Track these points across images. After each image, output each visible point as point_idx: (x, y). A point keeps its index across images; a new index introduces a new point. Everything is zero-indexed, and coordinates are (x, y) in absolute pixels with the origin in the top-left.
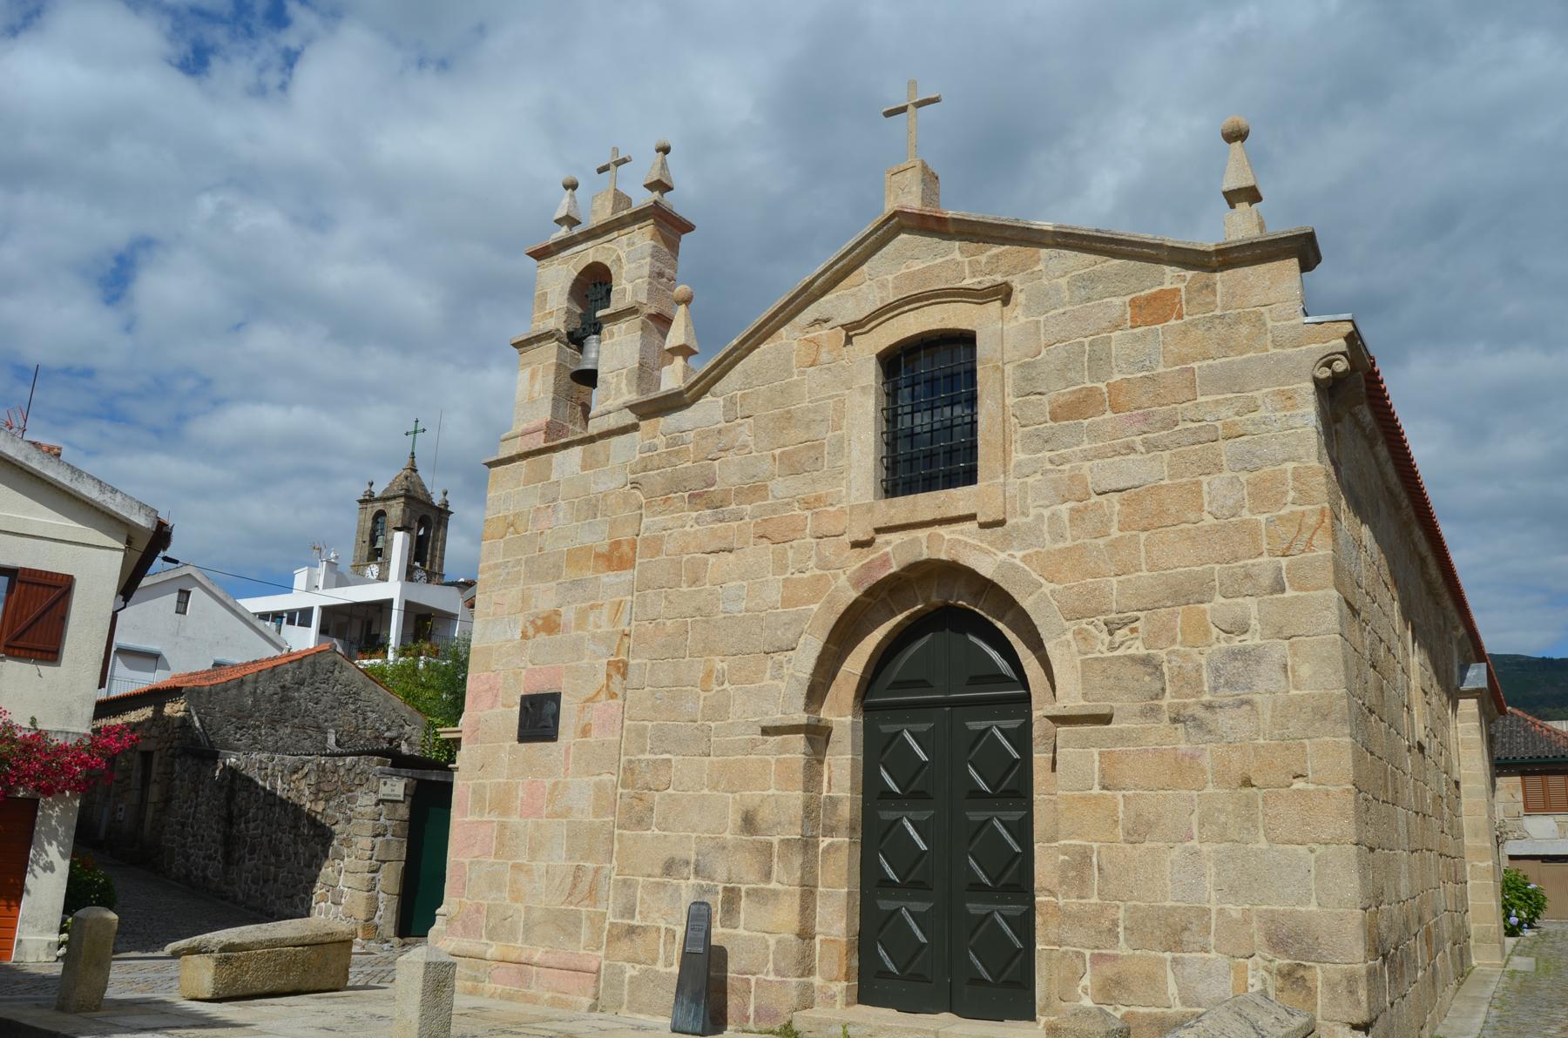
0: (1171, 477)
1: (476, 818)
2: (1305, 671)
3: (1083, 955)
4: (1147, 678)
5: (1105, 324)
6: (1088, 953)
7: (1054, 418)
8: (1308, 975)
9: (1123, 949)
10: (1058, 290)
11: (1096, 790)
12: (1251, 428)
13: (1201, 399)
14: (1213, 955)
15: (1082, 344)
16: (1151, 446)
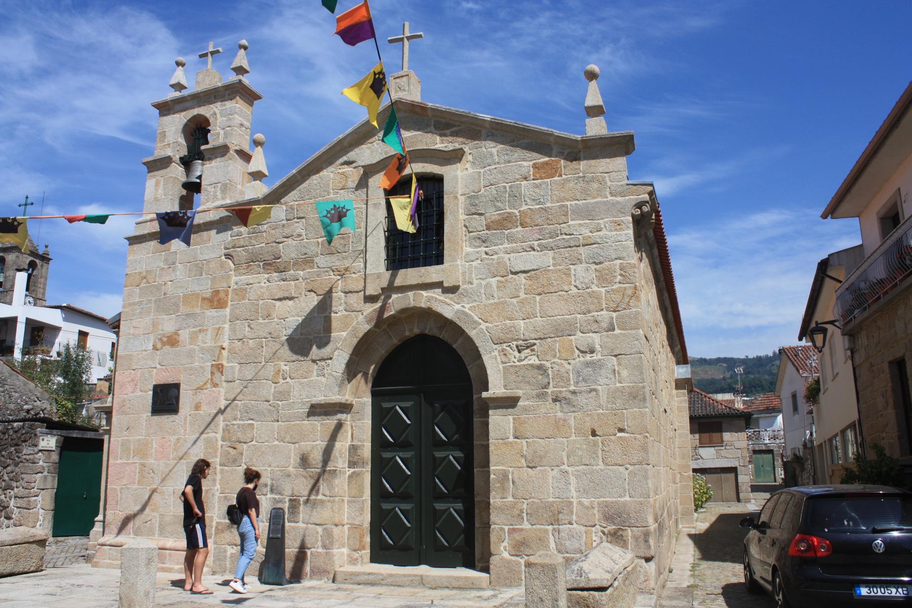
0: (554, 265)
1: (124, 461)
2: (625, 373)
3: (504, 529)
4: (540, 377)
5: (518, 177)
6: (506, 528)
7: (488, 228)
8: (624, 534)
9: (526, 525)
10: (492, 155)
11: (511, 439)
12: (599, 240)
13: (571, 223)
14: (575, 525)
15: (505, 187)
16: (544, 248)
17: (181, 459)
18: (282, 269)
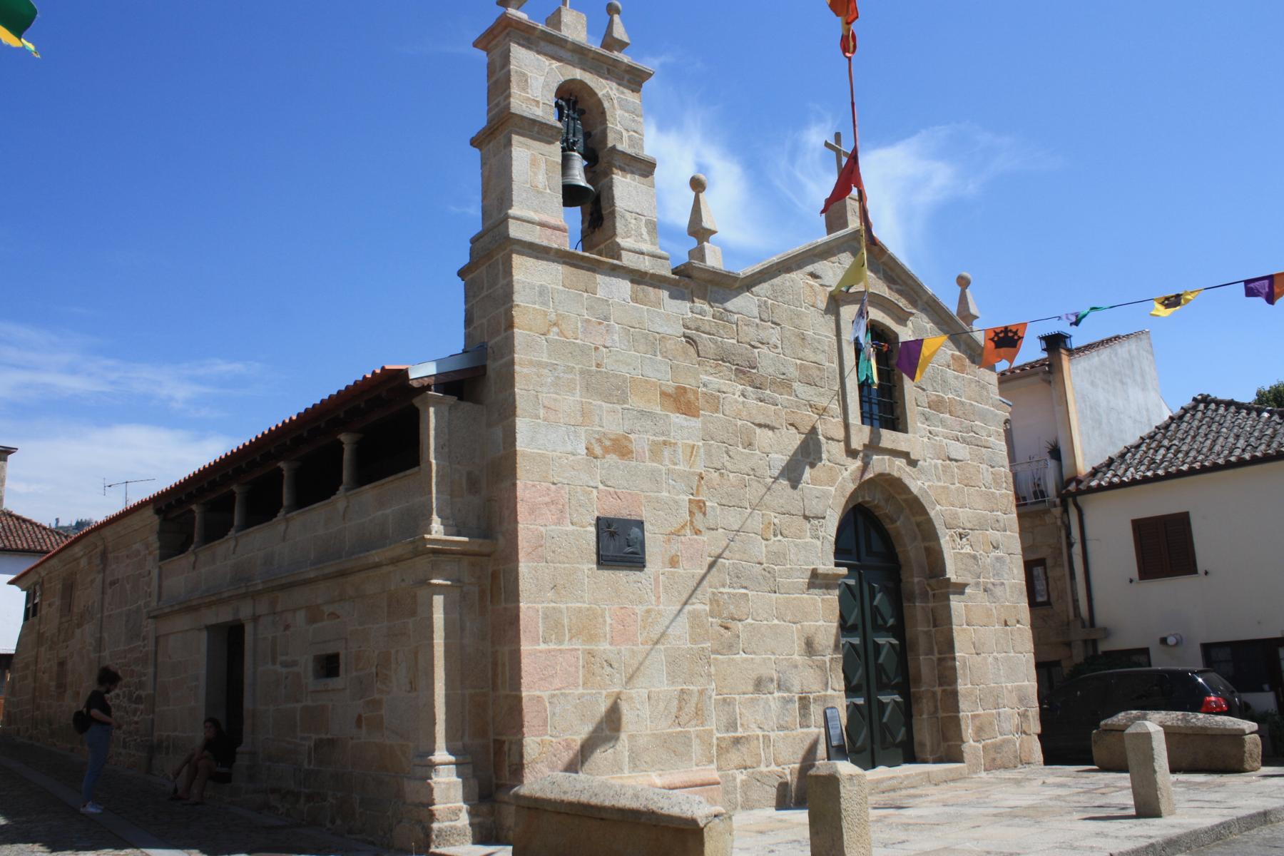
1: (552, 646)
17: (657, 643)
18: (757, 383)
